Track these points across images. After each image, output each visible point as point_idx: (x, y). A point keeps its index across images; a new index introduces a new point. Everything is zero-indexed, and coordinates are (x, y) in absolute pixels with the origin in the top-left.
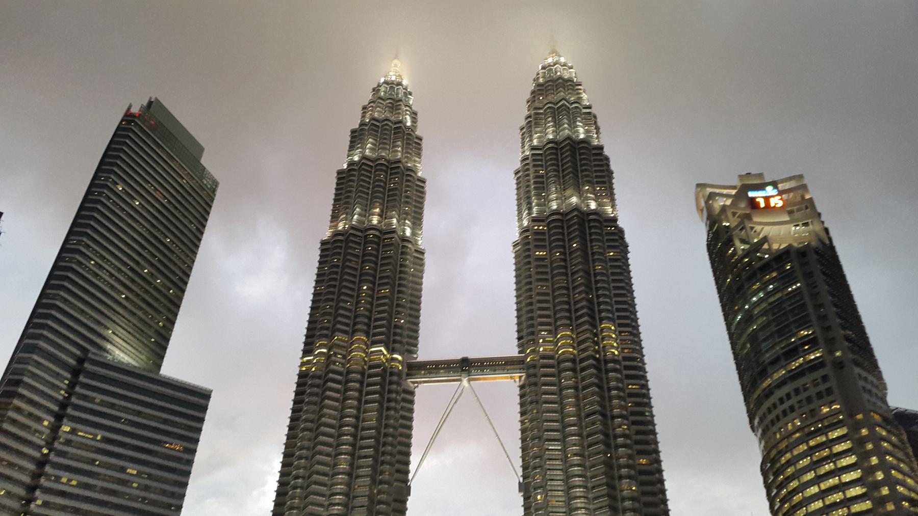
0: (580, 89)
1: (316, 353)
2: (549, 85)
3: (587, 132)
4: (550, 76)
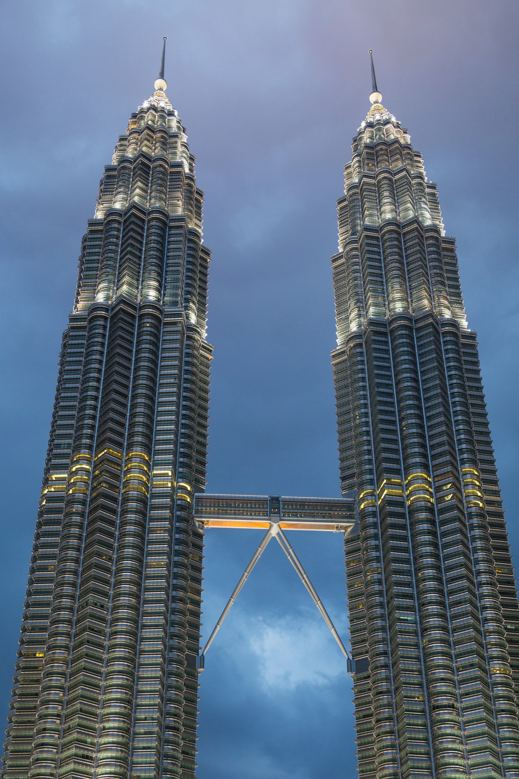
0: (419, 162)
1: (74, 469)
2: (381, 150)
3: (433, 218)
4: (380, 138)
